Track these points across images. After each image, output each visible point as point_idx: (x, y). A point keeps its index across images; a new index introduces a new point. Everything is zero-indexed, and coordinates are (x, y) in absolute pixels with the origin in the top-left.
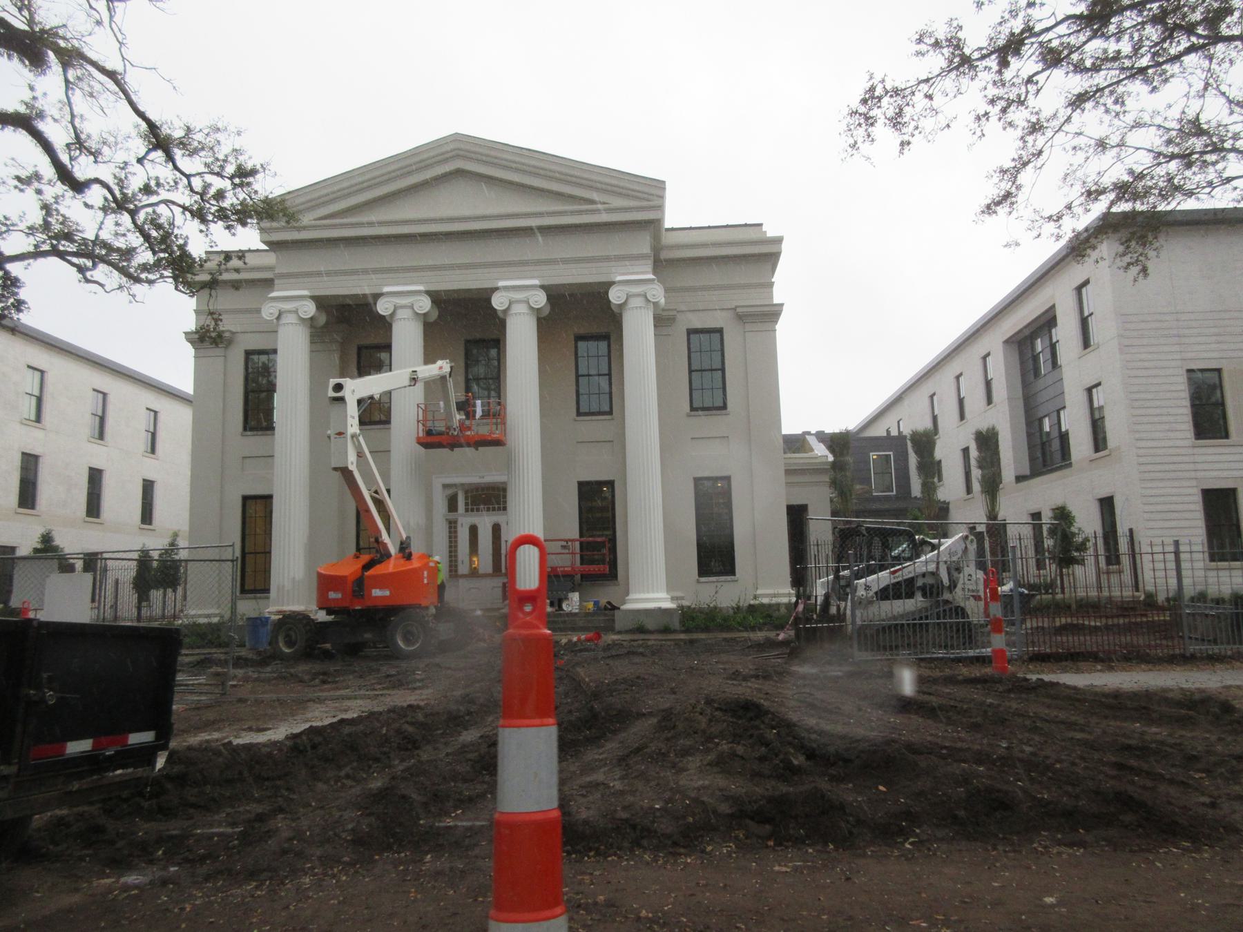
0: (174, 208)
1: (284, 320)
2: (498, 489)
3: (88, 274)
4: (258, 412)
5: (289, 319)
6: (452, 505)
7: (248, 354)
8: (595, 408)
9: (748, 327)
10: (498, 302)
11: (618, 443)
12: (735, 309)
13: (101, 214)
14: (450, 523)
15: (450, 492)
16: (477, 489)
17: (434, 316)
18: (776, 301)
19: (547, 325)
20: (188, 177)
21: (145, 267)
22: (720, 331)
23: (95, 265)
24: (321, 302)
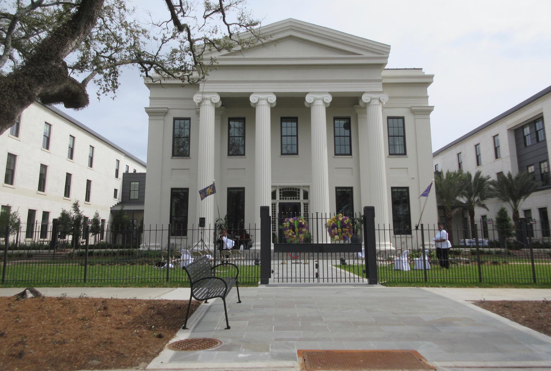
2: (296, 189)
4: (181, 146)
5: (208, 102)
7: (175, 119)
8: (343, 152)
9: (417, 117)
10: (253, 99)
12: (410, 108)
15: (274, 189)
16: (286, 189)
18: (429, 105)
22: (403, 118)
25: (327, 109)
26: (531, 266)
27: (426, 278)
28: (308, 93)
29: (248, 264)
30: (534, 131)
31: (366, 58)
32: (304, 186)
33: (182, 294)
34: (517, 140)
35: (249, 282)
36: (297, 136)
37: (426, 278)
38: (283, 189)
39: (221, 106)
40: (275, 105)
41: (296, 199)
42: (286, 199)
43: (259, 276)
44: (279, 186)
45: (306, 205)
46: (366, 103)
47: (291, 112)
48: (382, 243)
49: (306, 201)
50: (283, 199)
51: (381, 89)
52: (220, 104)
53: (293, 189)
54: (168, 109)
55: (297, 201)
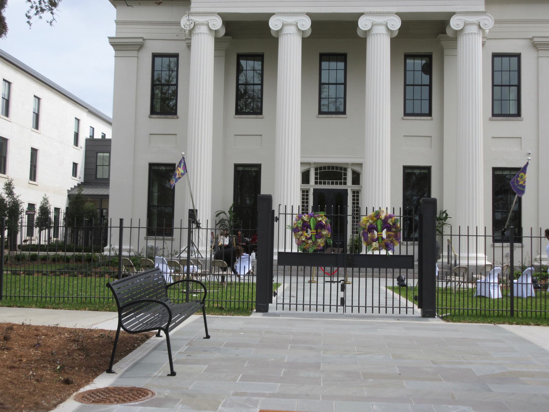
1: (197, 31)
2: (341, 168)
4: (164, 100)
6: (305, 178)
7: (155, 56)
8: (417, 111)
9: (541, 53)
12: (531, 39)
14: (303, 191)
15: (305, 168)
16: (325, 168)
22: (518, 56)
25: (393, 41)
27: (512, 311)
29: (246, 281)
32: (353, 164)
33: (107, 322)
35: (239, 309)
37: (512, 311)
38: (321, 168)
39: (226, 34)
41: (341, 183)
42: (325, 183)
43: (254, 300)
44: (315, 163)
45: (356, 194)
46: (366, 31)
49: (356, 187)
50: (320, 183)
51: (482, 8)
52: (223, 32)
53: (337, 168)
54: (144, 40)
55: (342, 187)
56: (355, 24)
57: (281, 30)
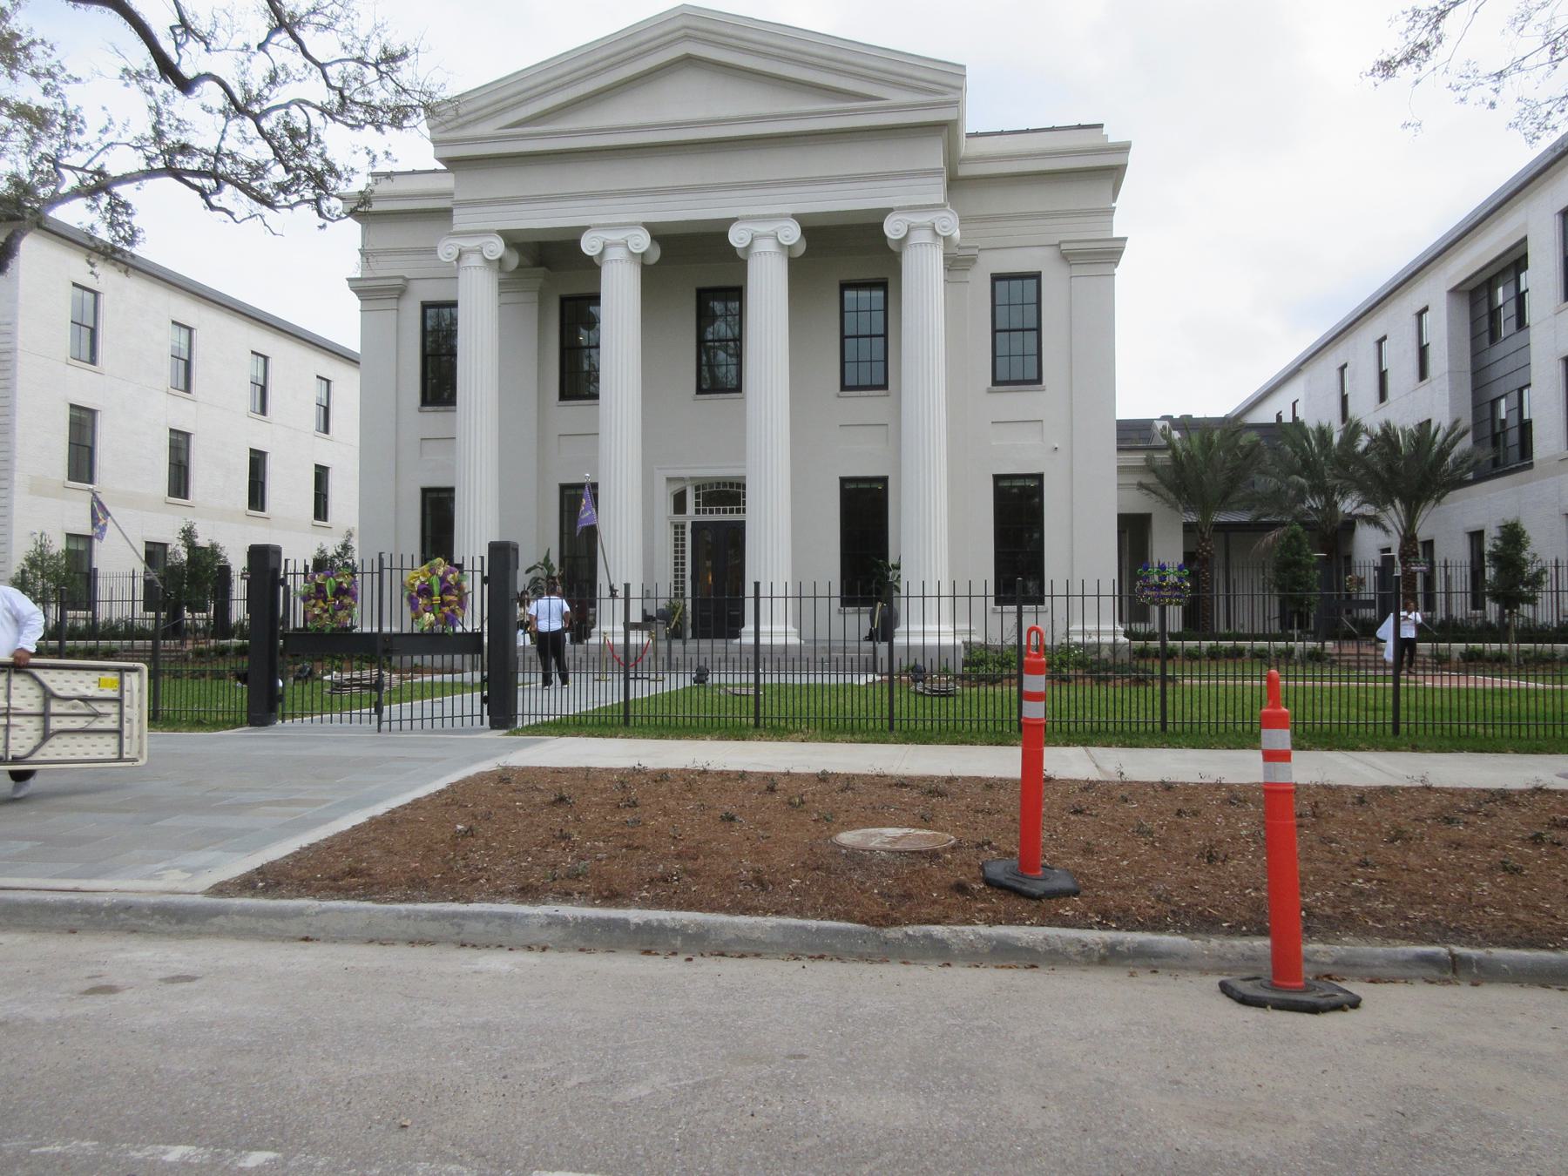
0: (307, 109)
1: (464, 263)
3: (214, 200)
5: (473, 260)
6: (679, 504)
7: (426, 306)
8: (865, 381)
9: (1076, 270)
11: (892, 430)
12: (1059, 245)
13: (221, 119)
14: (676, 527)
15: (677, 487)
16: (711, 486)
17: (655, 256)
18: (1116, 235)
19: (802, 270)
20: (322, 66)
21: (283, 188)
22: (1037, 276)
23: (219, 188)
24: (513, 240)
26: (1390, 692)
28: (586, 228)
30: (1512, 293)
31: (899, 106)
34: (1474, 322)
36: (885, 336)
40: (802, 249)
42: (711, 512)
44: (692, 478)
47: (698, 278)
48: (916, 627)
50: (704, 512)
51: (939, 197)
53: (732, 485)
54: (407, 280)
55: (734, 517)
56: (575, 244)
57: (602, 254)
